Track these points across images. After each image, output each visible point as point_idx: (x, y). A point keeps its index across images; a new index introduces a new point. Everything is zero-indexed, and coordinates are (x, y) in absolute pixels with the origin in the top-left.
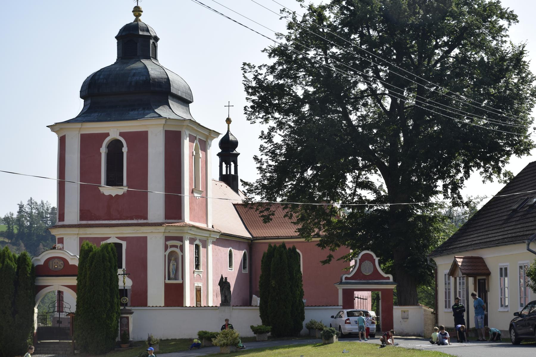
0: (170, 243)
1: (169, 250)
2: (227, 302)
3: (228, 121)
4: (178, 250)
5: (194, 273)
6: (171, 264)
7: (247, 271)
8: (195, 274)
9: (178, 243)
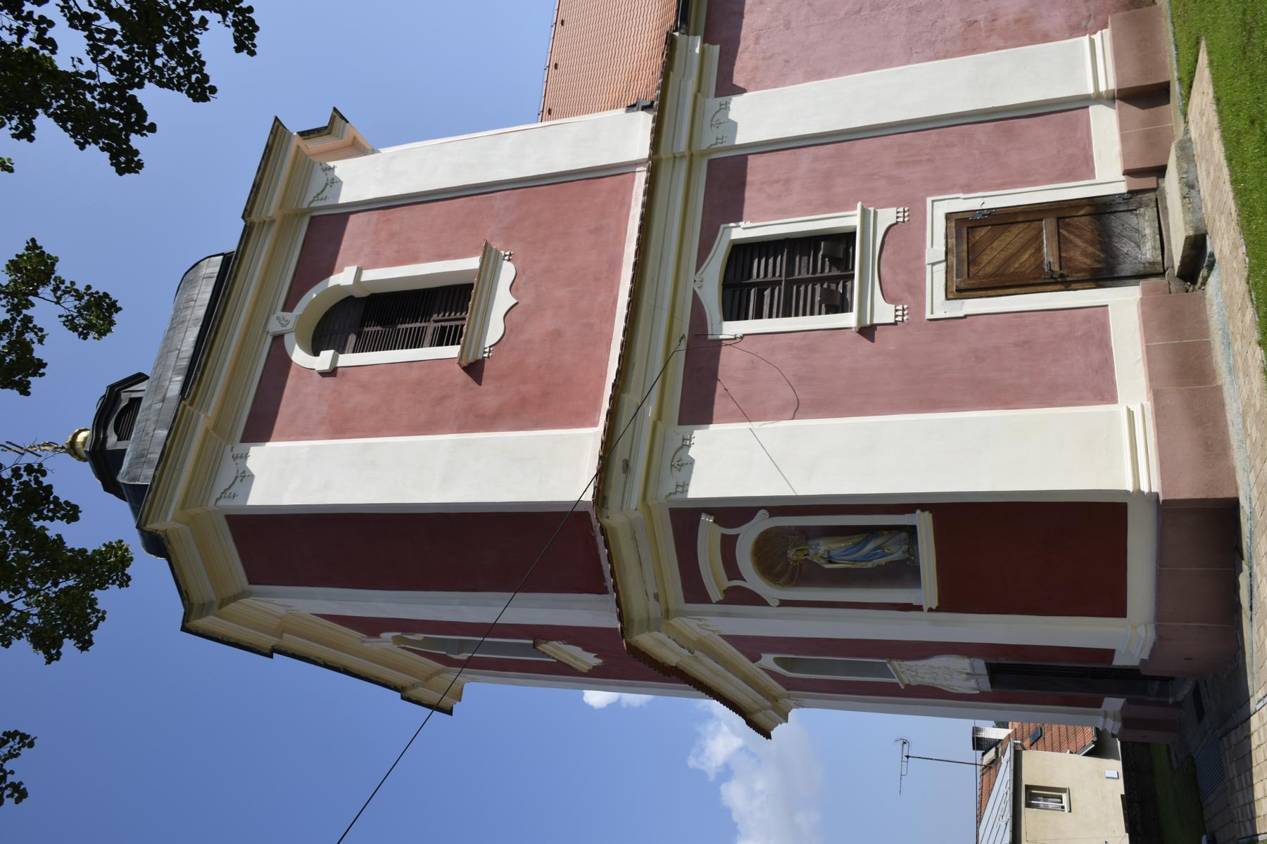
1: (753, 580)
4: (748, 535)
5: (867, 331)
8: (884, 312)
9: (709, 534)
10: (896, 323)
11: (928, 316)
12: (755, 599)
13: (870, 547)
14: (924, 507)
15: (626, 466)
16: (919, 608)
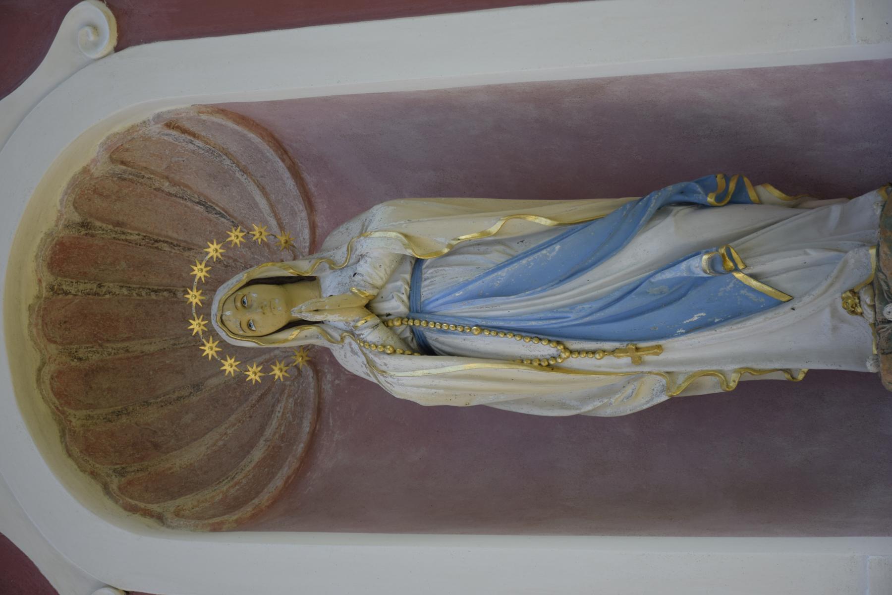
6: (413, 380)
13: (653, 244)
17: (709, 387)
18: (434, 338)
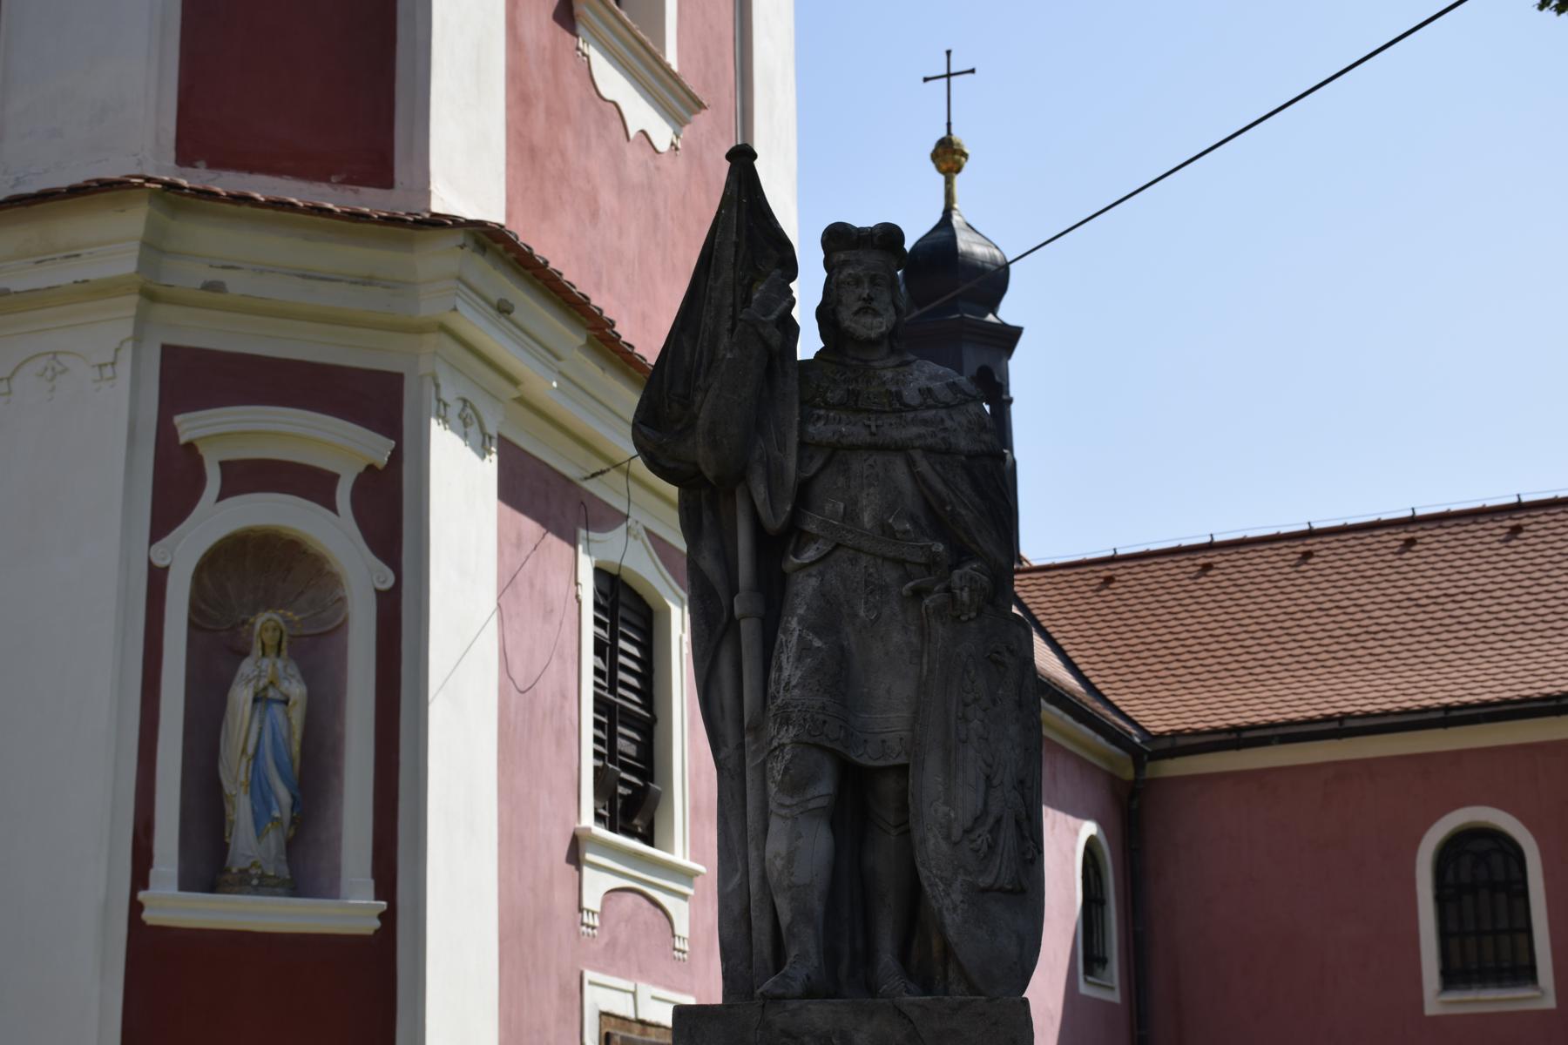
0: (219, 430)
1: (216, 519)
2: (925, 958)
3: (948, 156)
4: (332, 533)
5: (575, 856)
6: (241, 696)
7: (1110, 990)
8: (596, 885)
9: (343, 446)
10: (581, 910)
11: (589, 975)
12: (169, 510)
13: (283, 794)
14: (389, 919)
15: (504, 309)
16: (140, 877)
17: (228, 808)
18: (259, 705)
